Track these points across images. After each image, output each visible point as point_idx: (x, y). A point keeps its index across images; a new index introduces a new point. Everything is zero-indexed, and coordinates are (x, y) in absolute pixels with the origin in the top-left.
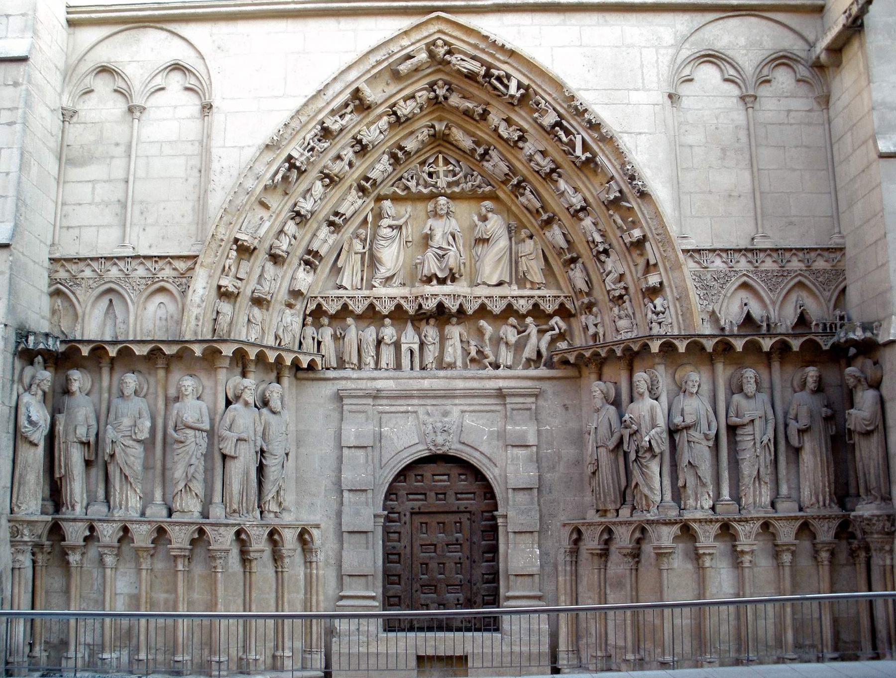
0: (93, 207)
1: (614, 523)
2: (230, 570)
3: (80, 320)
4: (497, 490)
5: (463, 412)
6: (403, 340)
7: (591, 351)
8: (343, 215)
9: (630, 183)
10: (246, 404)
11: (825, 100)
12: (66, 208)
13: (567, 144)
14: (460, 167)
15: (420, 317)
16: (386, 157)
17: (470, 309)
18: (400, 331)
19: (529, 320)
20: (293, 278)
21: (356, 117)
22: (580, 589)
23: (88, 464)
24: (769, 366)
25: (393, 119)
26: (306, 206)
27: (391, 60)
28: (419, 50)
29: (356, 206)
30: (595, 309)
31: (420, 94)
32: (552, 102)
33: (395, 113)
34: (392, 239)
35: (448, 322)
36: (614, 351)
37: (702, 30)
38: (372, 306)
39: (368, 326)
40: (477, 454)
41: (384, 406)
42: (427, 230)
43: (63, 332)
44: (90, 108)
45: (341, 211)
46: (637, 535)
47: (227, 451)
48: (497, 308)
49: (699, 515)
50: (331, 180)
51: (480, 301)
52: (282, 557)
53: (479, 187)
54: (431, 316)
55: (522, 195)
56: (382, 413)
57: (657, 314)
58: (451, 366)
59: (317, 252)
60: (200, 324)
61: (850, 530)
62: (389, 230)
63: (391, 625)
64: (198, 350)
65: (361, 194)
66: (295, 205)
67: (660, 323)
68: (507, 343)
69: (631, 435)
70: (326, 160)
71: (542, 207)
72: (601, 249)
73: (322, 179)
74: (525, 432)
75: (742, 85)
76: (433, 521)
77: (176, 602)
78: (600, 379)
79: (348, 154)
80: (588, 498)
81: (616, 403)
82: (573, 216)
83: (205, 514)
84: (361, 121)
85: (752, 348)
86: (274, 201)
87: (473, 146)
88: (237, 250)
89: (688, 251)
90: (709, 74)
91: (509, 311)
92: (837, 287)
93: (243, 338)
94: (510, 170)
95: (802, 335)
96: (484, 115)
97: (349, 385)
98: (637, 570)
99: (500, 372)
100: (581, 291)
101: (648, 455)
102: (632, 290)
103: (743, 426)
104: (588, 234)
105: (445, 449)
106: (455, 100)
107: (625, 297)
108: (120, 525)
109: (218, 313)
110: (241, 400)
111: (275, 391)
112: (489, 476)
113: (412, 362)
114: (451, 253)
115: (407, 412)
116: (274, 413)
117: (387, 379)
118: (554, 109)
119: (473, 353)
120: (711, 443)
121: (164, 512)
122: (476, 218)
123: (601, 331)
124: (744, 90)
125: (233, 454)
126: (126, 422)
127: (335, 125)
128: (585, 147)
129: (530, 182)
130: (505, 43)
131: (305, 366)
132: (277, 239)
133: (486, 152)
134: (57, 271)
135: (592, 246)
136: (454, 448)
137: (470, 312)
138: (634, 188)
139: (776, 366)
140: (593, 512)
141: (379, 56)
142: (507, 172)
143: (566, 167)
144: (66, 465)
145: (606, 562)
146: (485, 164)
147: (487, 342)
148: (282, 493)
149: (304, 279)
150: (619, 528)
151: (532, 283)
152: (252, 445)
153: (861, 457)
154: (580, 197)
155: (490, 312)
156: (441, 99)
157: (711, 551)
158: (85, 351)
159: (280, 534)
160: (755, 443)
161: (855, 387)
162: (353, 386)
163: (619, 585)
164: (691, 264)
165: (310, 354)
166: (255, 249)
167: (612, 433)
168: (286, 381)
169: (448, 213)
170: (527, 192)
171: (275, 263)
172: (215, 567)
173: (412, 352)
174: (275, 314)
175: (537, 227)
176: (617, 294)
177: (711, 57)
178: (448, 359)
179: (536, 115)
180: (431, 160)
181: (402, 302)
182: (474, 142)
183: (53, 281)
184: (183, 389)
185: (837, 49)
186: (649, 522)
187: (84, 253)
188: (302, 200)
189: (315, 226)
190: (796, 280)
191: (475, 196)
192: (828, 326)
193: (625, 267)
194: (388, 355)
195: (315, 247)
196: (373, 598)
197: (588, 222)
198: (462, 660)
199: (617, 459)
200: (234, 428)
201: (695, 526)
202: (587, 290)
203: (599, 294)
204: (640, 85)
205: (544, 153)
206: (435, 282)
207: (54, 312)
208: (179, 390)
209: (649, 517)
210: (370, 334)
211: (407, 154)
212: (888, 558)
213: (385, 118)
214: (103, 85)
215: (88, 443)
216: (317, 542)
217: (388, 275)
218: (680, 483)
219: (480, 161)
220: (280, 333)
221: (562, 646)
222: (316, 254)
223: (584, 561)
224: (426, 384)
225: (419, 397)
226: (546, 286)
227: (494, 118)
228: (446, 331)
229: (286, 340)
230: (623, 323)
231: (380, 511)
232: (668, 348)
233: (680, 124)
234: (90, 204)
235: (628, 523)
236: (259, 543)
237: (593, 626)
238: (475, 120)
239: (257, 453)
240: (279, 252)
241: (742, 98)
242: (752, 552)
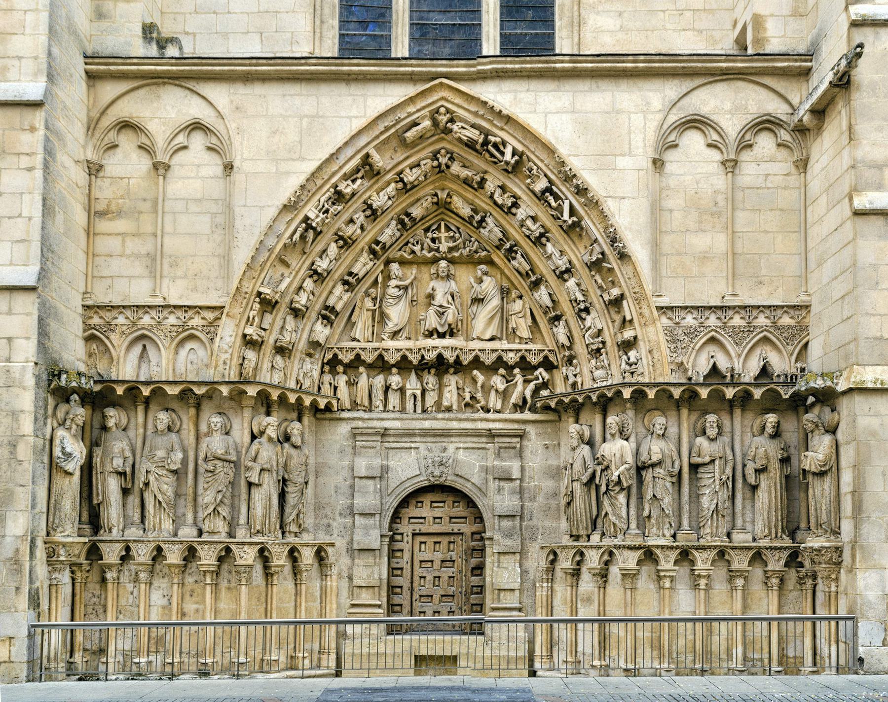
0: (124, 259)
1: (586, 547)
2: (254, 583)
3: (115, 362)
4: (485, 515)
5: (458, 448)
6: (408, 386)
7: (570, 397)
8: (357, 275)
9: (612, 246)
10: (270, 439)
11: (803, 165)
12: (97, 259)
13: (555, 209)
14: (460, 233)
15: (422, 367)
16: (394, 223)
17: (466, 360)
18: (405, 378)
19: (516, 371)
20: (311, 331)
21: (367, 184)
22: (555, 604)
23: (125, 492)
24: (731, 414)
25: (400, 185)
26: (322, 265)
27: (398, 127)
28: (423, 118)
29: (368, 267)
30: (575, 361)
31: (424, 162)
32: (544, 168)
33: (402, 180)
34: (399, 297)
35: (446, 372)
36: (590, 397)
37: (690, 95)
38: (381, 356)
39: (379, 374)
40: (469, 485)
41: (391, 443)
42: (429, 290)
43: (99, 374)
44: (115, 165)
45: (355, 270)
46: (606, 557)
47: (252, 480)
48: (488, 360)
49: (662, 542)
50: (345, 243)
51: (474, 353)
52: (300, 573)
53: (476, 252)
54: (432, 367)
55: (514, 258)
56: (389, 448)
57: (631, 365)
58: (449, 409)
59: (333, 308)
60: (227, 367)
61: (799, 560)
62: (397, 290)
63: (393, 629)
64: (225, 390)
65: (372, 256)
66: (313, 264)
67: (632, 373)
68: (497, 391)
69: (602, 471)
70: (340, 223)
71: (531, 270)
72: (582, 307)
73: (336, 241)
74: (511, 467)
75: (724, 150)
76: (430, 541)
77: (204, 612)
78: (577, 422)
79: (360, 218)
80: (564, 525)
81: (590, 443)
82: (558, 277)
83: (231, 535)
84: (371, 186)
85: (717, 396)
86: (294, 260)
87: (471, 213)
88: (260, 303)
89: (662, 308)
90: (693, 141)
91: (500, 362)
92: (800, 342)
93: (268, 381)
94: (504, 235)
95: (764, 385)
96: (482, 183)
97: (360, 424)
98: (605, 588)
99: (490, 416)
100: (563, 346)
101: (617, 488)
102: (609, 343)
103: (704, 465)
104: (572, 293)
105: (442, 479)
106: (455, 168)
107: (602, 351)
108: (153, 545)
109: (244, 358)
110: (265, 436)
111: (295, 429)
112: (479, 504)
113: (415, 405)
114: (450, 311)
115: (410, 448)
116: (295, 447)
117: (393, 419)
118: (546, 175)
119: (468, 399)
120: (674, 480)
121: (195, 532)
122: (472, 280)
123: (579, 380)
124: (725, 155)
125: (257, 482)
126: (161, 454)
127: (346, 188)
128: (573, 211)
129: (521, 247)
130: (502, 109)
131: (322, 406)
132: (297, 294)
133: (483, 220)
134: (91, 318)
135: (575, 304)
136: (450, 480)
137: (465, 363)
138: (615, 250)
139: (738, 412)
141: (388, 122)
142: (502, 237)
143: (554, 231)
144: (104, 493)
145: (578, 580)
146: (482, 230)
147: (480, 389)
149: (321, 332)
150: (590, 551)
151: (520, 338)
152: (275, 474)
153: (814, 495)
154: (565, 259)
155: (483, 363)
156: (443, 167)
157: (671, 574)
158: (120, 390)
159: (299, 552)
161: (812, 432)
162: (365, 425)
163: (588, 600)
164: (664, 320)
165: (327, 397)
166: (277, 302)
167: (586, 469)
168: (306, 420)
169: (448, 276)
170: (519, 256)
171: (296, 316)
172: (240, 581)
173: (415, 397)
174: (296, 362)
175: (527, 288)
176: (594, 347)
177: (696, 123)
178: (446, 403)
179: (529, 181)
180: (434, 227)
181: (407, 353)
182: (472, 209)
183: (87, 327)
184: (213, 425)
185: (820, 112)
186: (615, 546)
187: (117, 302)
188: (318, 259)
189: (331, 284)
190: (761, 335)
191: (472, 261)
192: (789, 377)
193: (604, 323)
194: (394, 400)
195: (331, 302)
196: (379, 606)
197: (571, 283)
198: (454, 659)
199: (589, 490)
200: (259, 460)
202: (568, 344)
203: (580, 349)
204: (627, 150)
205: (534, 219)
206: (435, 336)
207: (90, 355)
208: (209, 426)
209: (616, 542)
210: (379, 381)
211: (413, 220)
212: (833, 584)
213: (393, 185)
214: (127, 141)
215: (125, 474)
216: (332, 559)
217: (395, 329)
218: (646, 513)
219: (477, 228)
220: (301, 378)
221: (538, 652)
222: (332, 309)
223: (559, 579)
224: (427, 424)
225: (421, 436)
226: (532, 340)
227: (490, 186)
228: (445, 380)
229: (307, 384)
230: (598, 373)
231: (386, 531)
232: (639, 395)
233: (661, 190)
234: (121, 256)
235: (598, 547)
236: (280, 560)
237: (563, 633)
238: (473, 188)
239: (279, 481)
240: (297, 306)
241: (723, 163)
242: (709, 576)
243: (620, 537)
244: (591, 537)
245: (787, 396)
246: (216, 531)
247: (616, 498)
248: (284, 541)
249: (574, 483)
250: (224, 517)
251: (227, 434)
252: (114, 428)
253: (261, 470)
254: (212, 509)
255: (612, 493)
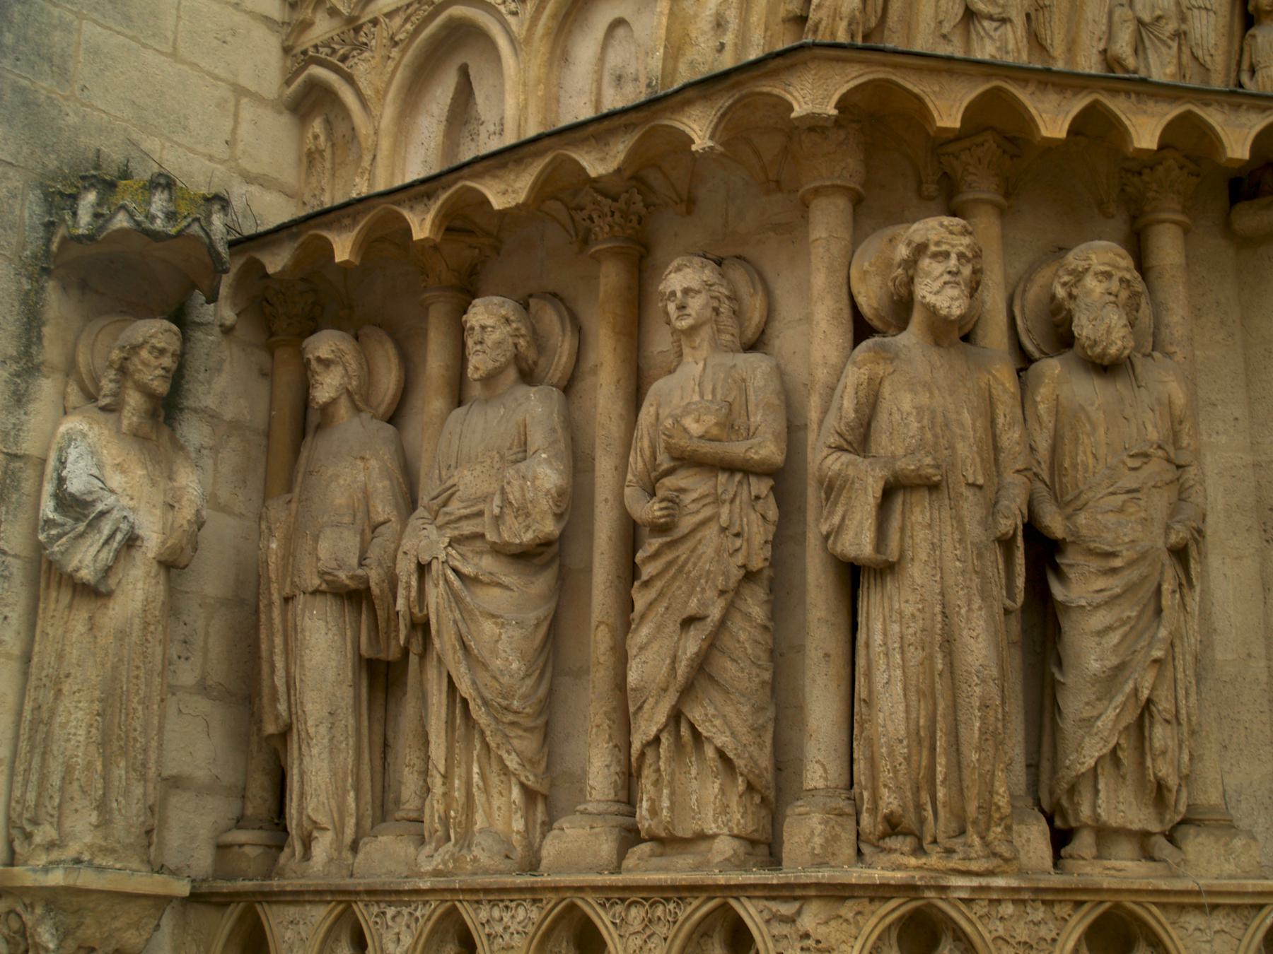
110: (917, 317)
148: (1160, 735)
152: (971, 508)
200: (883, 443)
220: (1123, 46)
239: (1006, 544)
246: (685, 829)
248: (1056, 880)
250: (721, 754)
251: (755, 345)
252: (343, 410)
253: (889, 493)
254: (661, 717)
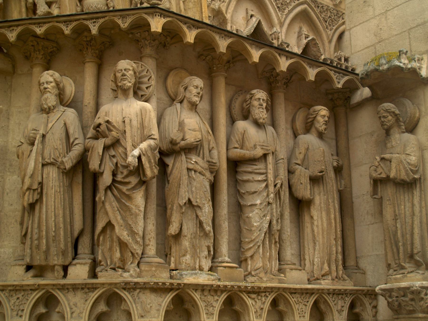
1: (63, 288)
69: (106, 148)
101: (134, 180)
103: (252, 160)
140: (21, 270)
150: (70, 295)
160: (267, 186)
199: (71, 186)
201: (197, 296)
209: (127, 277)
218: (173, 229)
243: (132, 268)
244: (71, 270)
245: (340, 86)
247: (129, 198)
249: (46, 170)
255: (124, 189)
